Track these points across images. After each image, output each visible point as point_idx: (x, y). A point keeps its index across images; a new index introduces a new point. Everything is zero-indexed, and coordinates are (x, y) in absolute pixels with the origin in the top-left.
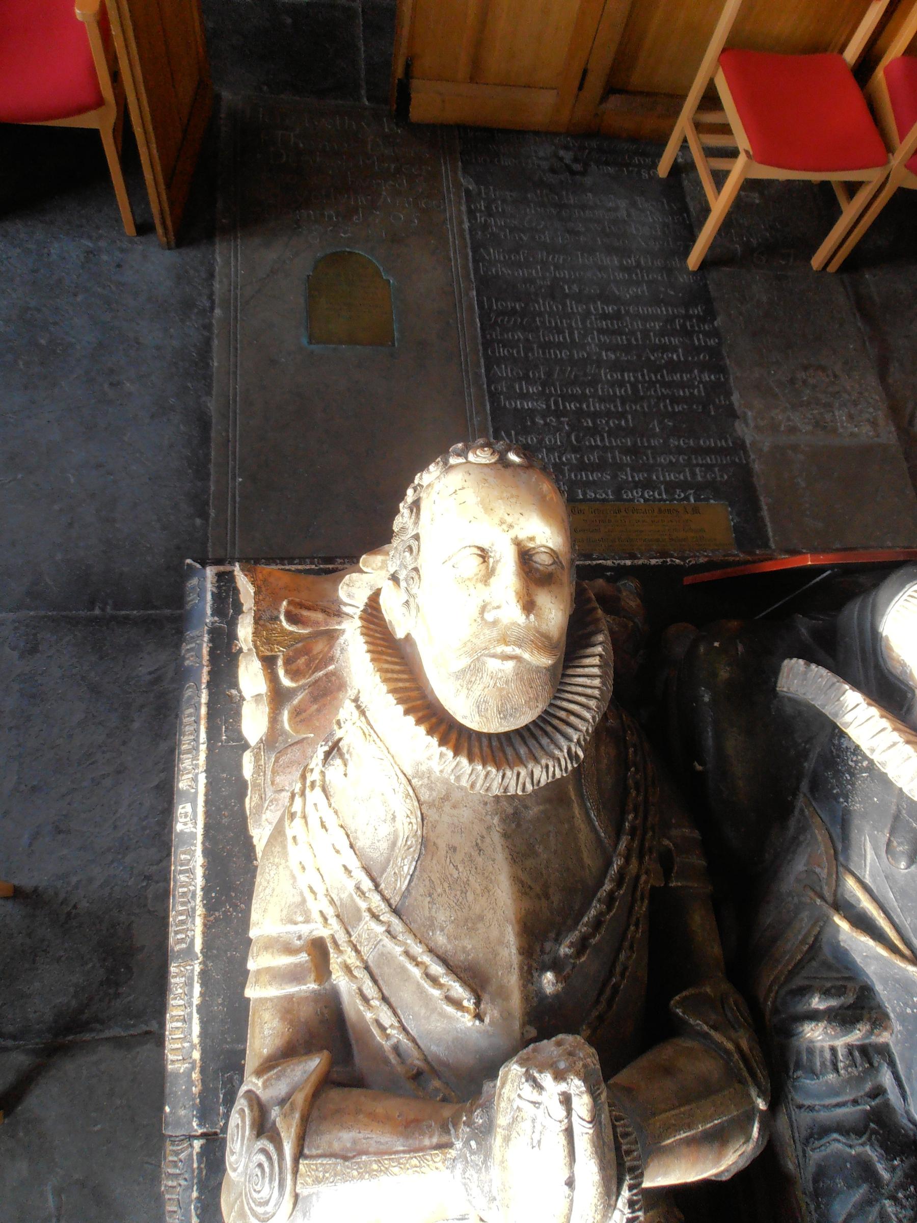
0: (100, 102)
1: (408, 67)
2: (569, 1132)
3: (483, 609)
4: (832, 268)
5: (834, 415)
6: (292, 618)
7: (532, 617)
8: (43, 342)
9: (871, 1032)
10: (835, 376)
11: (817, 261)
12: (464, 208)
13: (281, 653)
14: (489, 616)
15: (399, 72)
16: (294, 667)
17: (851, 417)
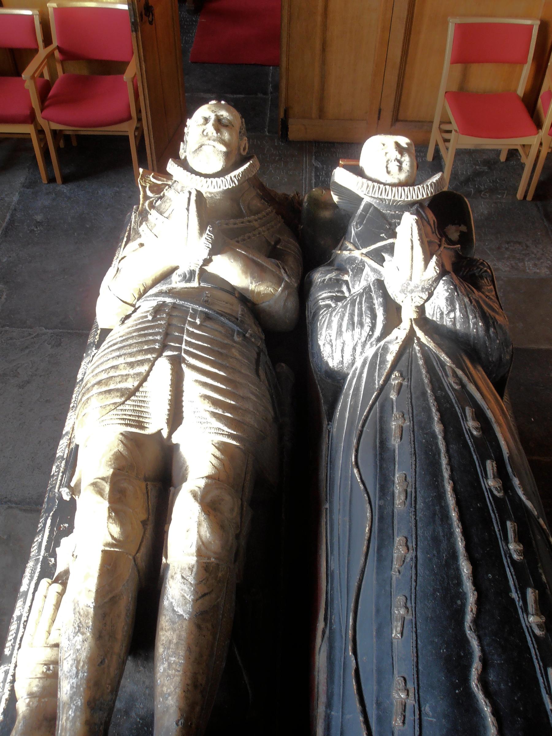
0: (130, 118)
1: (286, 111)
2: (189, 199)
3: (203, 131)
4: (529, 198)
5: (525, 264)
6: (153, 177)
7: (219, 134)
8: (88, 226)
9: (340, 274)
10: (527, 246)
11: (519, 195)
12: (313, 174)
13: (148, 185)
14: (205, 133)
15: (282, 115)
16: (152, 189)
17: (535, 265)
